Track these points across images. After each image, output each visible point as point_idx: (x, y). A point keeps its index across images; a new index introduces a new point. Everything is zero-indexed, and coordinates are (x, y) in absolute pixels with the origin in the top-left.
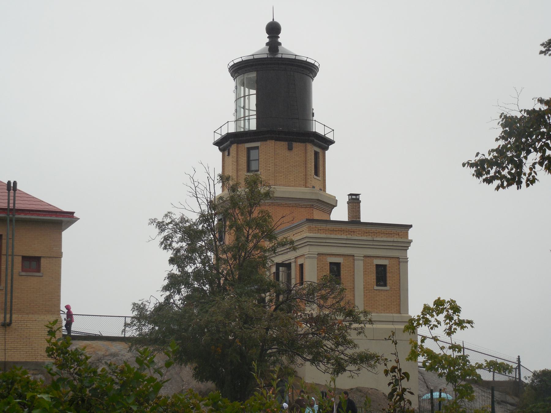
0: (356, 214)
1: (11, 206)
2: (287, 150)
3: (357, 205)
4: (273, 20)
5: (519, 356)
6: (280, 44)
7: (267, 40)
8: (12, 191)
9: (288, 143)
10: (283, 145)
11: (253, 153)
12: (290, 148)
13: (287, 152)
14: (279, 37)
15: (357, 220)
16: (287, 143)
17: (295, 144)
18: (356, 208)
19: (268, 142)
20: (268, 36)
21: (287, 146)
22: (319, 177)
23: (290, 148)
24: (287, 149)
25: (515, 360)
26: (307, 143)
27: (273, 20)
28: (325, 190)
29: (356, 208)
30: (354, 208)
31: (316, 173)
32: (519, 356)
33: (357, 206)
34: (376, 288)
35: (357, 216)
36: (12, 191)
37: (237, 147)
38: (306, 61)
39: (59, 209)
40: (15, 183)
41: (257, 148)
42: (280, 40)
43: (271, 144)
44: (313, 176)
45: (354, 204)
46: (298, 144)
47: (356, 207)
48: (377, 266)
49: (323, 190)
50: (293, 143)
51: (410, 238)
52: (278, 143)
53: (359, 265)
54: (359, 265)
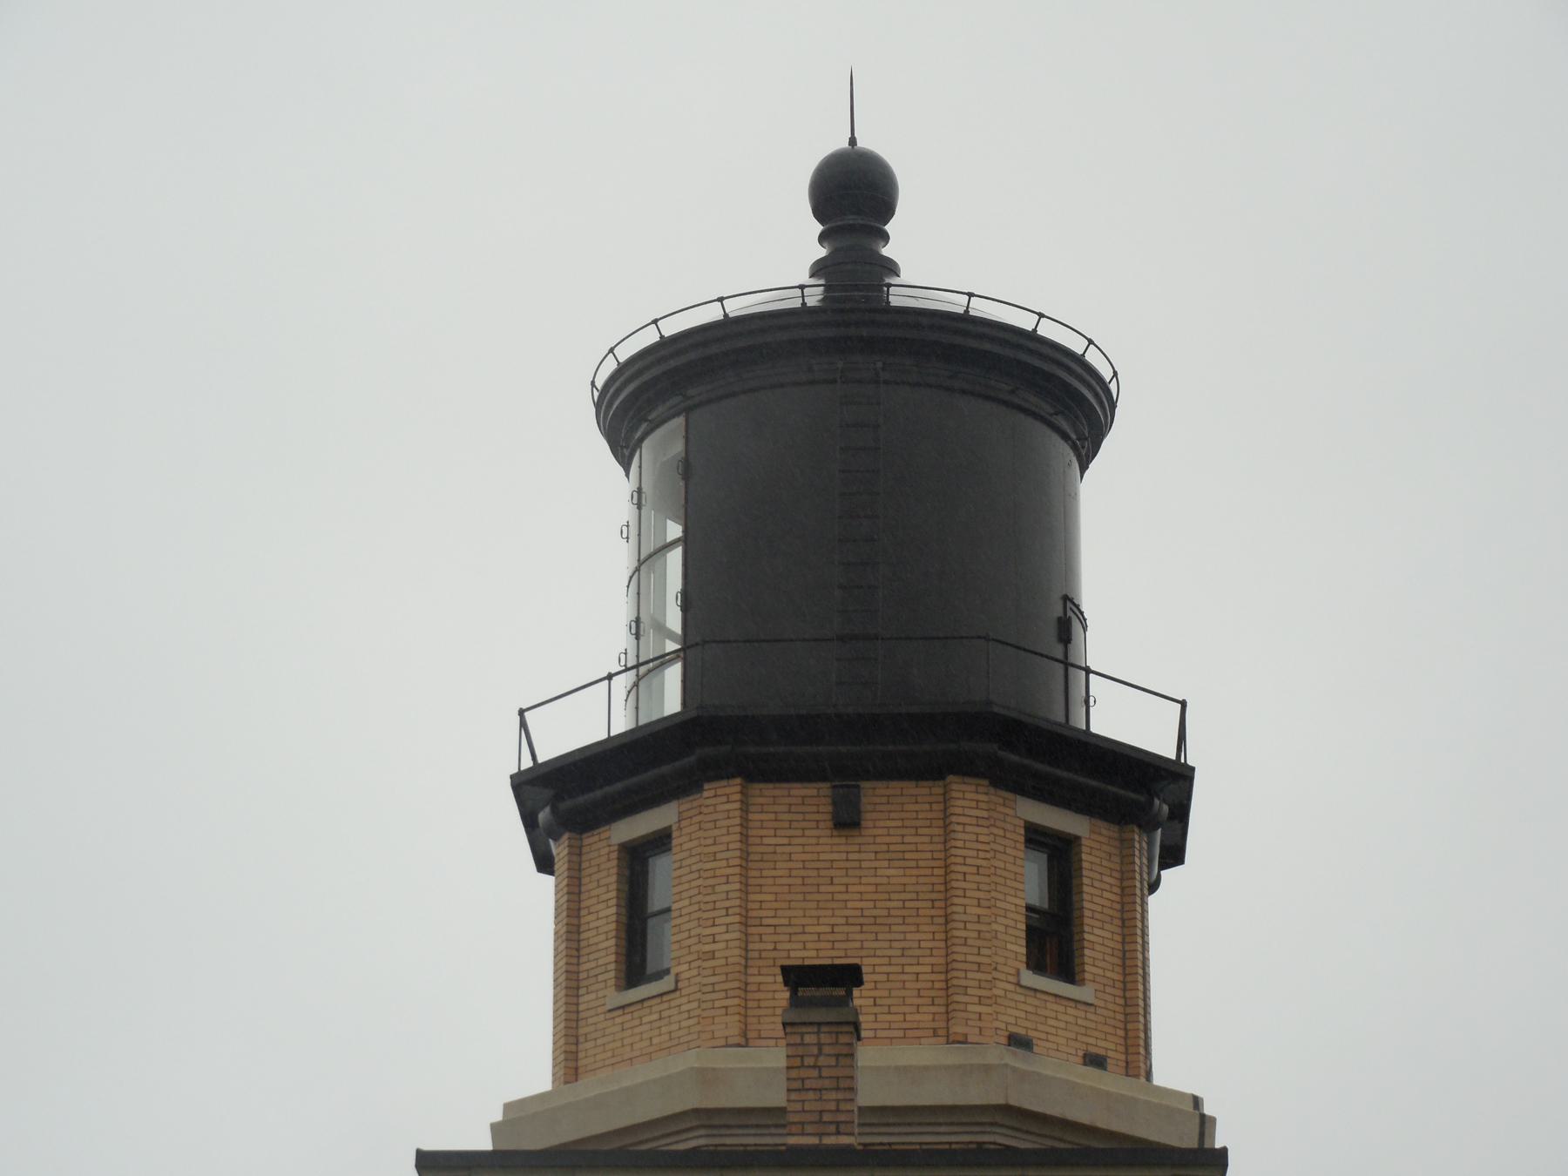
0: (818, 1106)
2: (828, 832)
3: (825, 1039)
4: (853, 141)
6: (891, 268)
10: (813, 798)
11: (664, 875)
12: (847, 820)
13: (829, 841)
14: (885, 237)
15: (830, 1141)
16: (825, 788)
17: (876, 796)
18: (822, 1061)
19: (709, 790)
20: (819, 228)
21: (830, 808)
23: (847, 820)
24: (830, 824)
27: (853, 141)
29: (822, 1061)
30: (809, 1061)
33: (827, 1050)
35: (826, 1118)
37: (576, 852)
38: (966, 318)
41: (661, 841)
42: (886, 251)
44: (1018, 973)
45: (809, 1039)
46: (896, 786)
47: (820, 1053)
49: (1115, 1056)
50: (865, 785)
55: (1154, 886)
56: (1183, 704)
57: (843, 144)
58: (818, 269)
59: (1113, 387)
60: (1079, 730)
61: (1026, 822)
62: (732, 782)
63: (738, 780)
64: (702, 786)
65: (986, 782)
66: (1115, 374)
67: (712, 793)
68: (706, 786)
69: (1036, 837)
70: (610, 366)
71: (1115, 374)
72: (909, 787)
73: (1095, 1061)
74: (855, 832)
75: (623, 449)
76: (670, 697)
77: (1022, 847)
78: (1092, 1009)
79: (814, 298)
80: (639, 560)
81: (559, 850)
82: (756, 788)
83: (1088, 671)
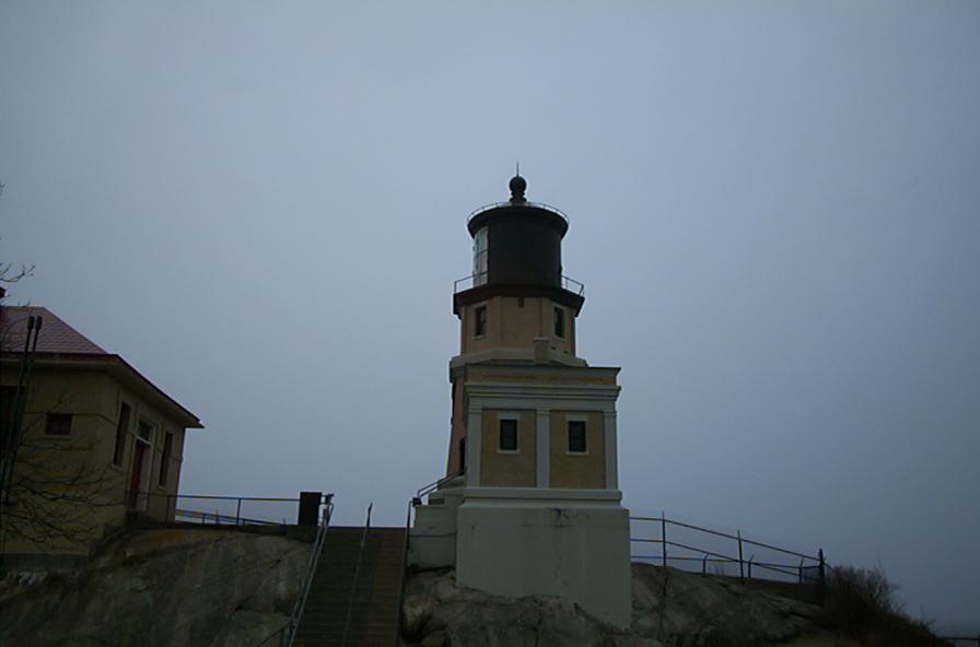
1: (30, 350)
5: (821, 551)
7: (511, 196)
8: (34, 330)
10: (515, 300)
12: (521, 305)
23: (521, 305)
25: (817, 556)
28: (574, 354)
31: (559, 332)
32: (821, 551)
34: (568, 453)
36: (34, 330)
39: (100, 349)
40: (40, 319)
41: (484, 308)
43: (497, 300)
48: (571, 423)
51: (618, 384)
52: (507, 299)
53: (543, 424)
54: (543, 424)
56: (583, 286)
58: (511, 200)
63: (499, 297)
69: (556, 309)
73: (566, 352)
75: (473, 236)
76: (484, 281)
79: (510, 204)
81: (463, 310)
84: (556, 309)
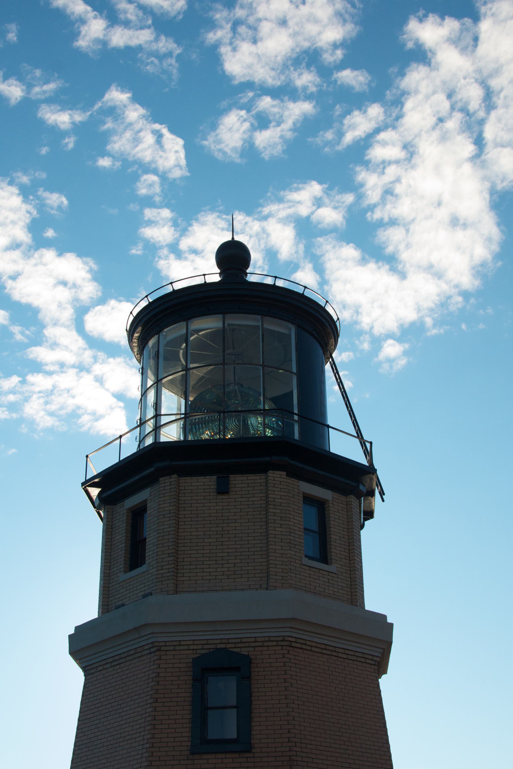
9: (217, 477)
21: (215, 487)
22: (331, 564)
26: (270, 473)
50: (232, 477)
55: (362, 527)
57: (230, 239)
59: (337, 323)
60: (326, 451)
61: (304, 493)
62: (172, 476)
63: (175, 476)
64: (159, 480)
65: (285, 473)
66: (338, 319)
67: (163, 481)
68: (161, 479)
70: (132, 318)
71: (338, 319)
72: (252, 477)
74: (227, 497)
77: (302, 502)
78: (336, 576)
80: (141, 395)
82: (183, 480)
83: (328, 427)
84: (308, 499)
